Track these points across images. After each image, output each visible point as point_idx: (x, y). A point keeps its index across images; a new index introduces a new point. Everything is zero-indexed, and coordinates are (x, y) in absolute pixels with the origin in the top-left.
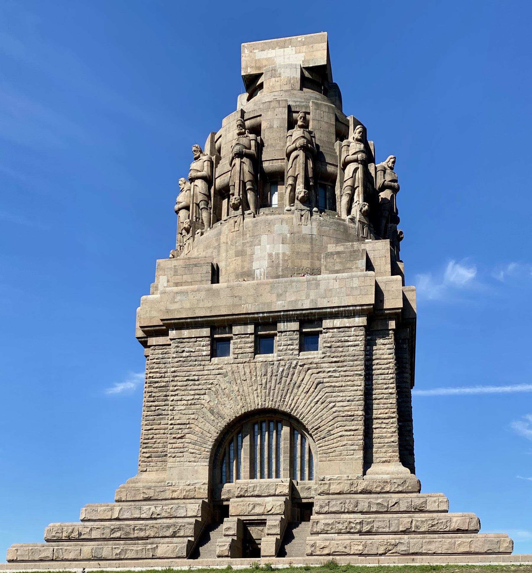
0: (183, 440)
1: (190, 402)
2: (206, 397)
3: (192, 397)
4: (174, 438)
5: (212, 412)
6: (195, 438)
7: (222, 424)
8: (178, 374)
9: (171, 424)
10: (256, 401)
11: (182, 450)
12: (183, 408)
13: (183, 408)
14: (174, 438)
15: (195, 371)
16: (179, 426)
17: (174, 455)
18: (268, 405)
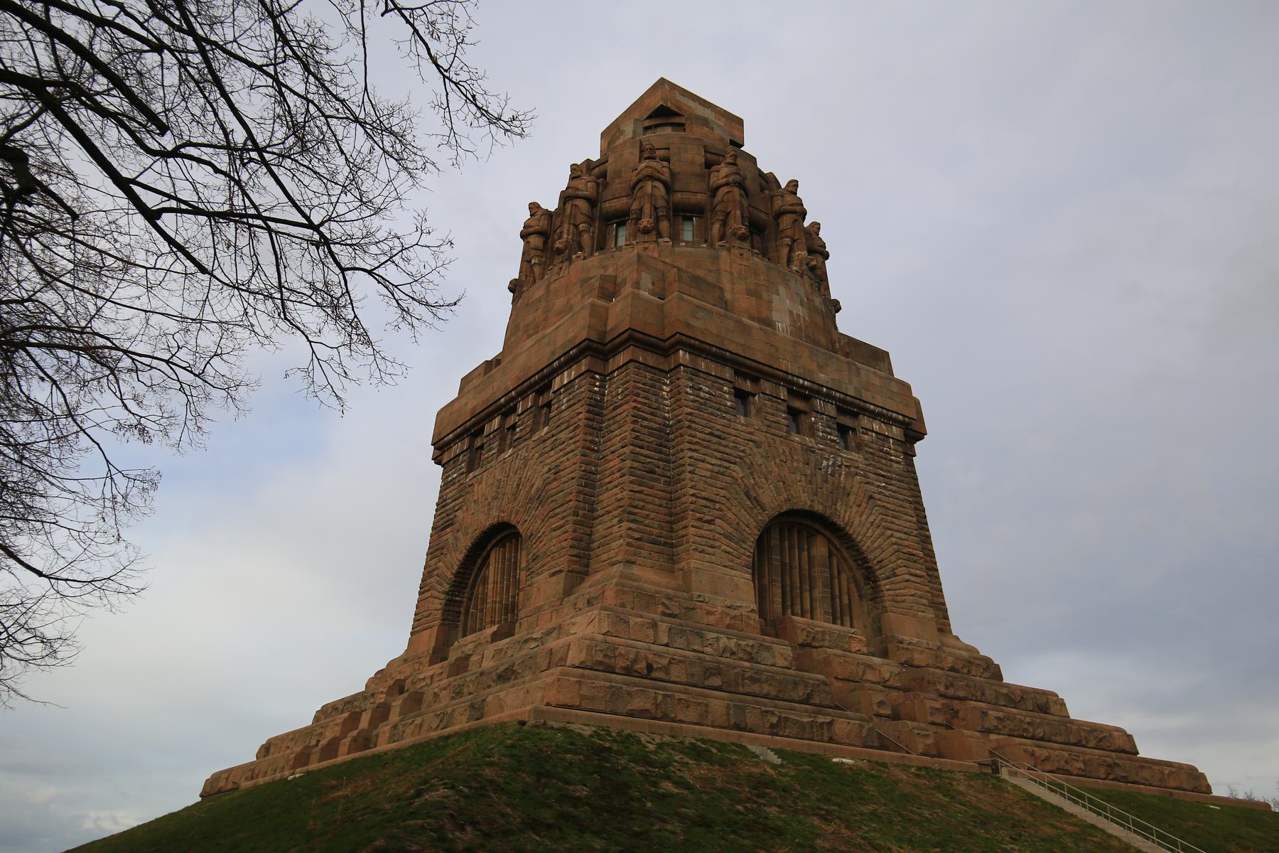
0: (712, 527)
1: (716, 469)
2: (737, 468)
3: (719, 462)
4: (700, 519)
5: (747, 494)
6: (730, 530)
7: (764, 518)
8: (697, 420)
9: (693, 495)
10: (804, 500)
11: (711, 542)
12: (708, 474)
13: (708, 474)
14: (700, 519)
15: (719, 424)
16: (704, 502)
17: (701, 548)
18: (819, 508)
